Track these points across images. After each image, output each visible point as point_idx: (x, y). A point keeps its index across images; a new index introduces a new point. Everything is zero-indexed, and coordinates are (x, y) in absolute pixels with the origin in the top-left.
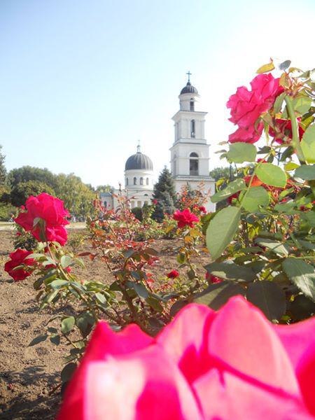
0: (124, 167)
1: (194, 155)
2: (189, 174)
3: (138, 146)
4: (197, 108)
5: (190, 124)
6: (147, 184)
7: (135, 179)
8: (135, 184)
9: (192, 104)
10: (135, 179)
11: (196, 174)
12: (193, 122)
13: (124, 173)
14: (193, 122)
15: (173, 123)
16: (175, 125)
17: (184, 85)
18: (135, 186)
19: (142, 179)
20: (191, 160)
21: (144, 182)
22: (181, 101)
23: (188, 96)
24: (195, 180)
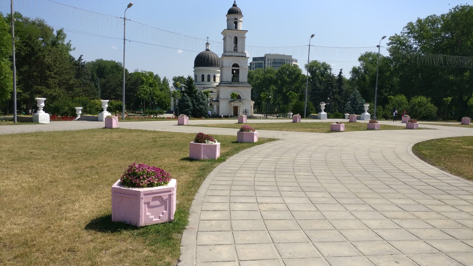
0: (193, 65)
1: (235, 65)
2: (230, 80)
3: (207, 44)
4: (241, 27)
5: (233, 40)
6: (215, 80)
7: (203, 76)
8: (203, 80)
9: (236, 23)
10: (203, 76)
11: (238, 81)
12: (236, 39)
13: (193, 70)
14: (236, 39)
15: (222, 37)
16: (223, 39)
17: (231, 6)
18: (203, 83)
19: (209, 76)
20: (233, 70)
21: (212, 79)
22: (227, 20)
23: (233, 16)
24: (235, 85)
